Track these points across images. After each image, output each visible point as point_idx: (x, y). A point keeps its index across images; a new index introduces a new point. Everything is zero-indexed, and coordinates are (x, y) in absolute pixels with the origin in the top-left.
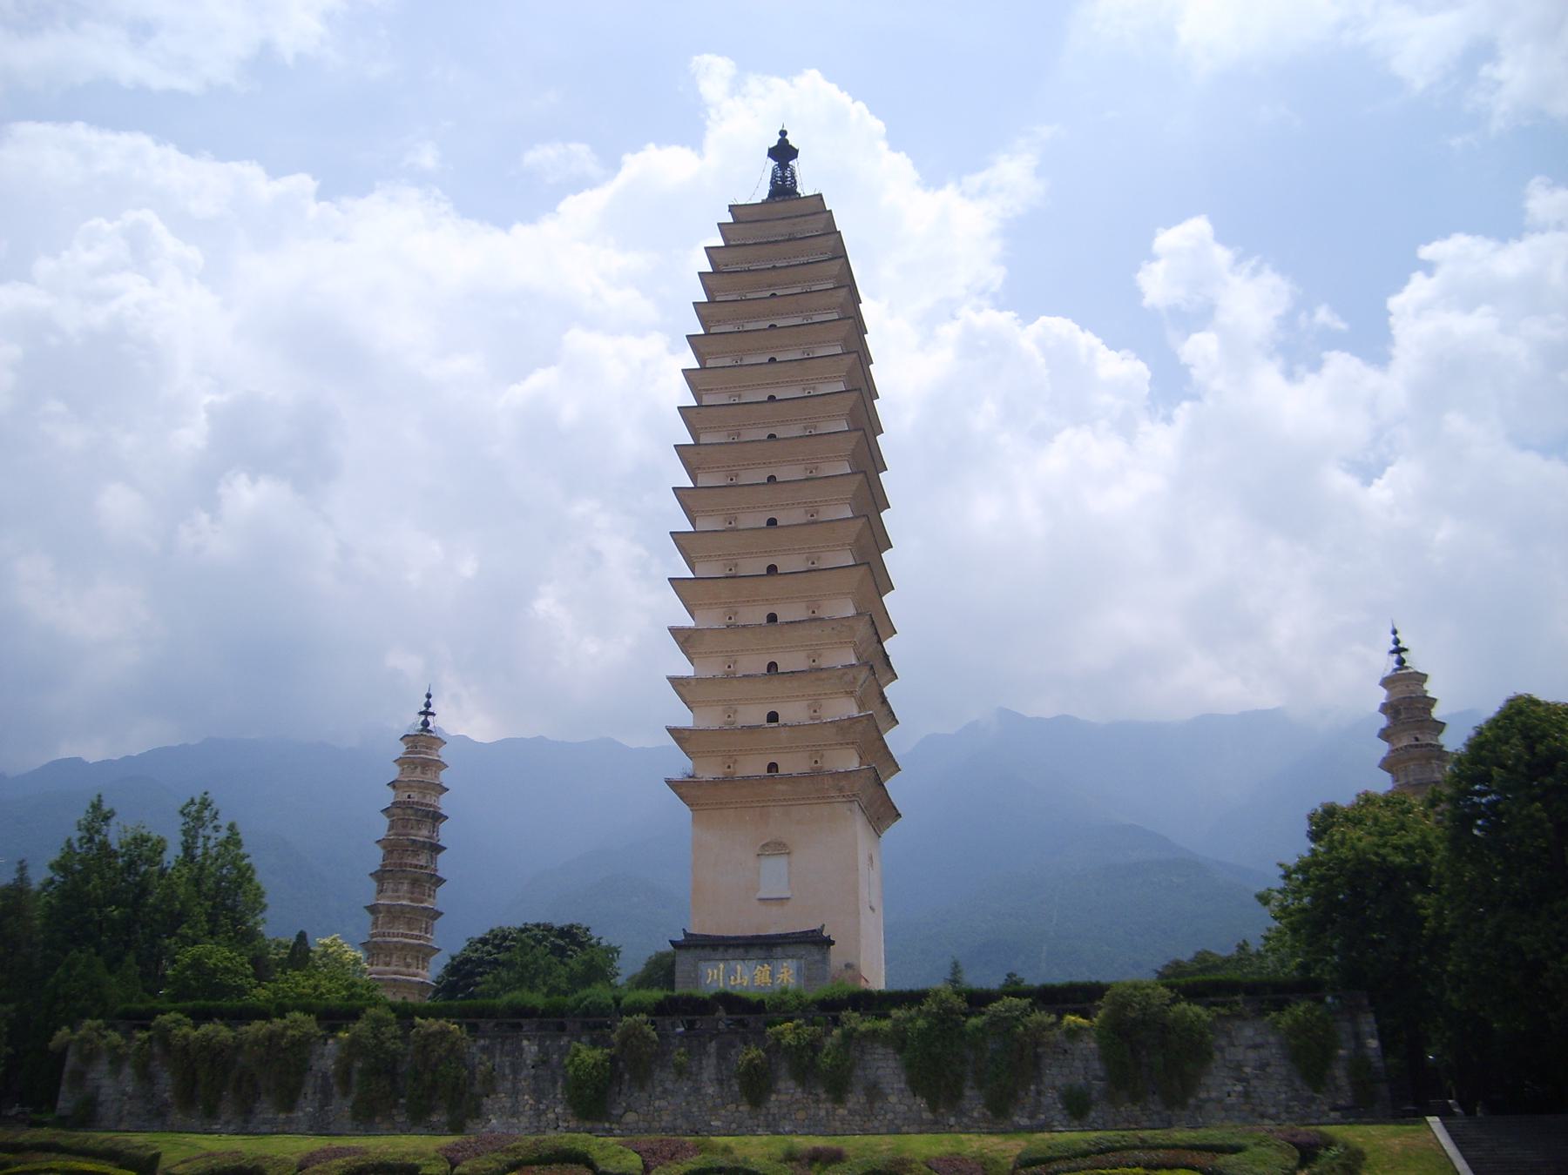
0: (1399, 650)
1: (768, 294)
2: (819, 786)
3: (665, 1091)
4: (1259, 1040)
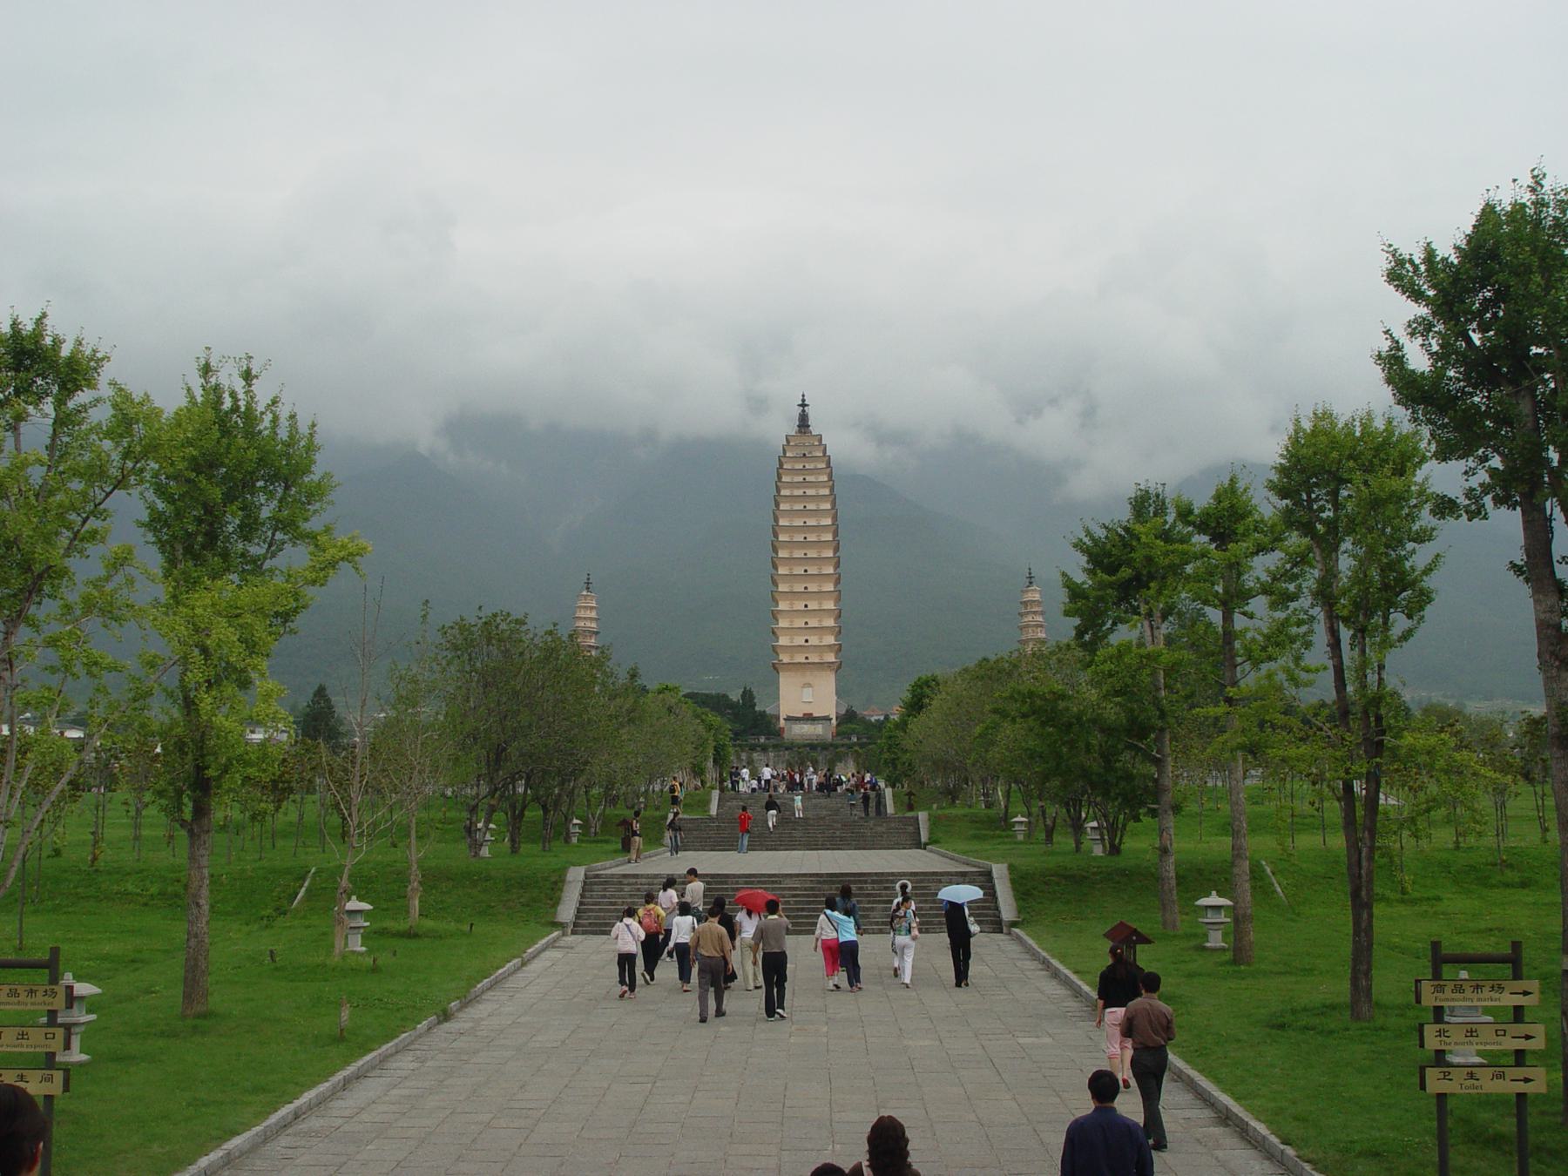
2: (821, 666)
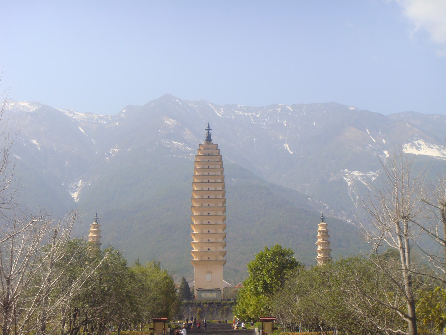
1: (207, 167)
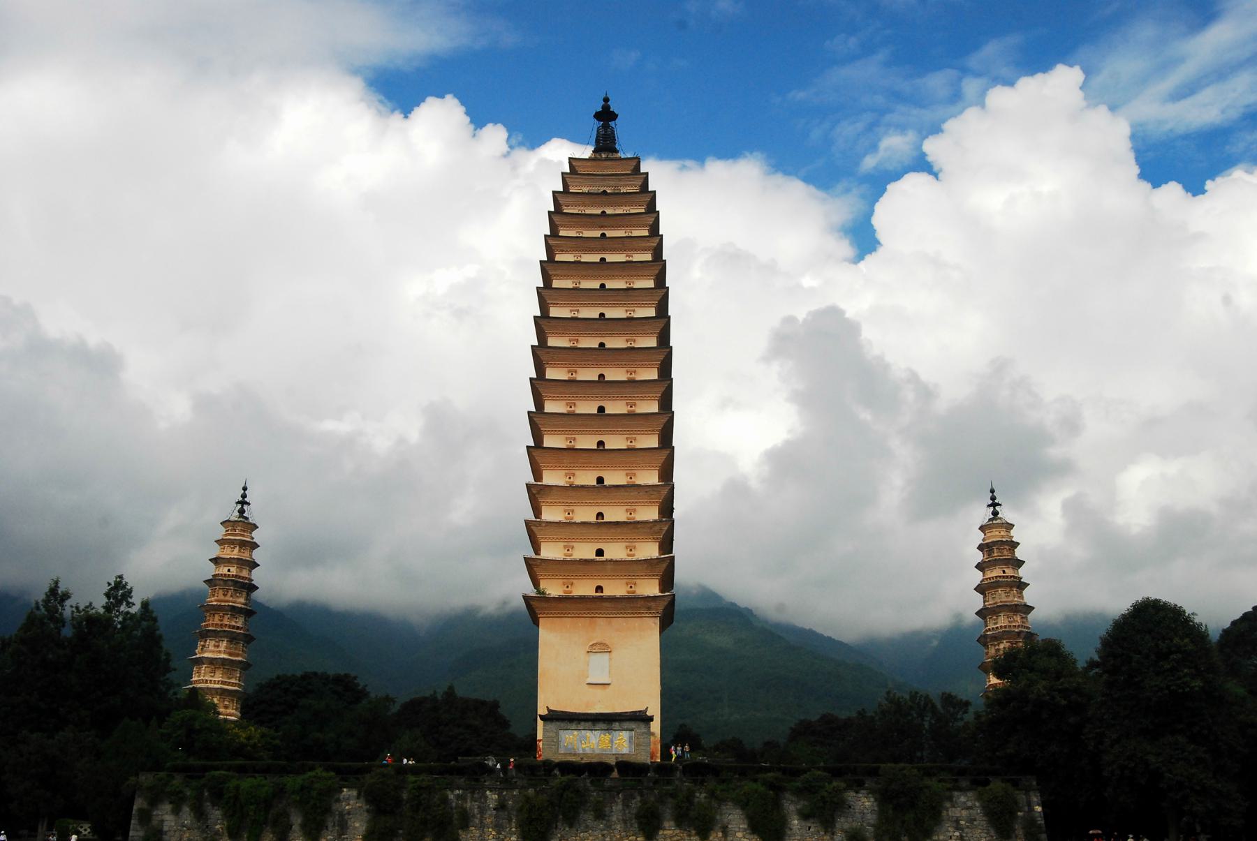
0: (994, 505)
2: (631, 605)
3: (587, 827)
4: (969, 804)
